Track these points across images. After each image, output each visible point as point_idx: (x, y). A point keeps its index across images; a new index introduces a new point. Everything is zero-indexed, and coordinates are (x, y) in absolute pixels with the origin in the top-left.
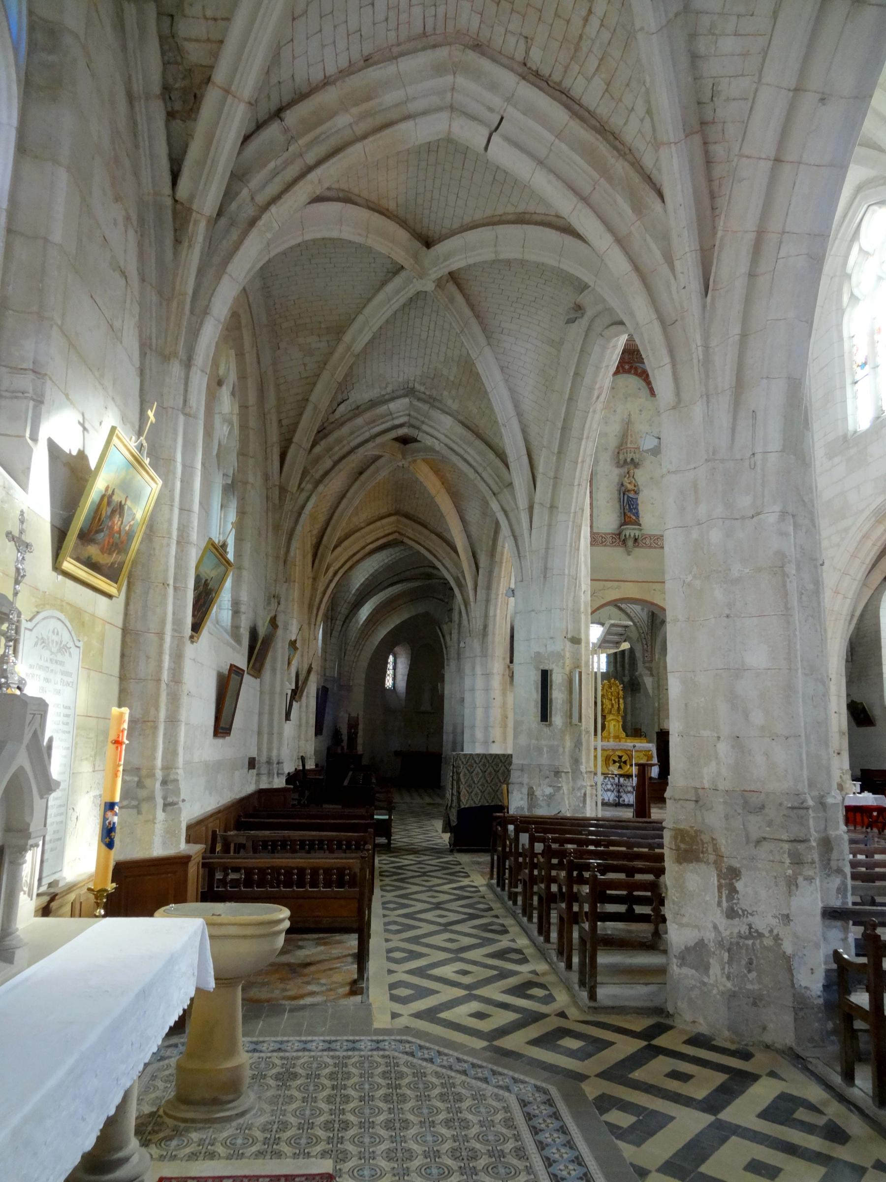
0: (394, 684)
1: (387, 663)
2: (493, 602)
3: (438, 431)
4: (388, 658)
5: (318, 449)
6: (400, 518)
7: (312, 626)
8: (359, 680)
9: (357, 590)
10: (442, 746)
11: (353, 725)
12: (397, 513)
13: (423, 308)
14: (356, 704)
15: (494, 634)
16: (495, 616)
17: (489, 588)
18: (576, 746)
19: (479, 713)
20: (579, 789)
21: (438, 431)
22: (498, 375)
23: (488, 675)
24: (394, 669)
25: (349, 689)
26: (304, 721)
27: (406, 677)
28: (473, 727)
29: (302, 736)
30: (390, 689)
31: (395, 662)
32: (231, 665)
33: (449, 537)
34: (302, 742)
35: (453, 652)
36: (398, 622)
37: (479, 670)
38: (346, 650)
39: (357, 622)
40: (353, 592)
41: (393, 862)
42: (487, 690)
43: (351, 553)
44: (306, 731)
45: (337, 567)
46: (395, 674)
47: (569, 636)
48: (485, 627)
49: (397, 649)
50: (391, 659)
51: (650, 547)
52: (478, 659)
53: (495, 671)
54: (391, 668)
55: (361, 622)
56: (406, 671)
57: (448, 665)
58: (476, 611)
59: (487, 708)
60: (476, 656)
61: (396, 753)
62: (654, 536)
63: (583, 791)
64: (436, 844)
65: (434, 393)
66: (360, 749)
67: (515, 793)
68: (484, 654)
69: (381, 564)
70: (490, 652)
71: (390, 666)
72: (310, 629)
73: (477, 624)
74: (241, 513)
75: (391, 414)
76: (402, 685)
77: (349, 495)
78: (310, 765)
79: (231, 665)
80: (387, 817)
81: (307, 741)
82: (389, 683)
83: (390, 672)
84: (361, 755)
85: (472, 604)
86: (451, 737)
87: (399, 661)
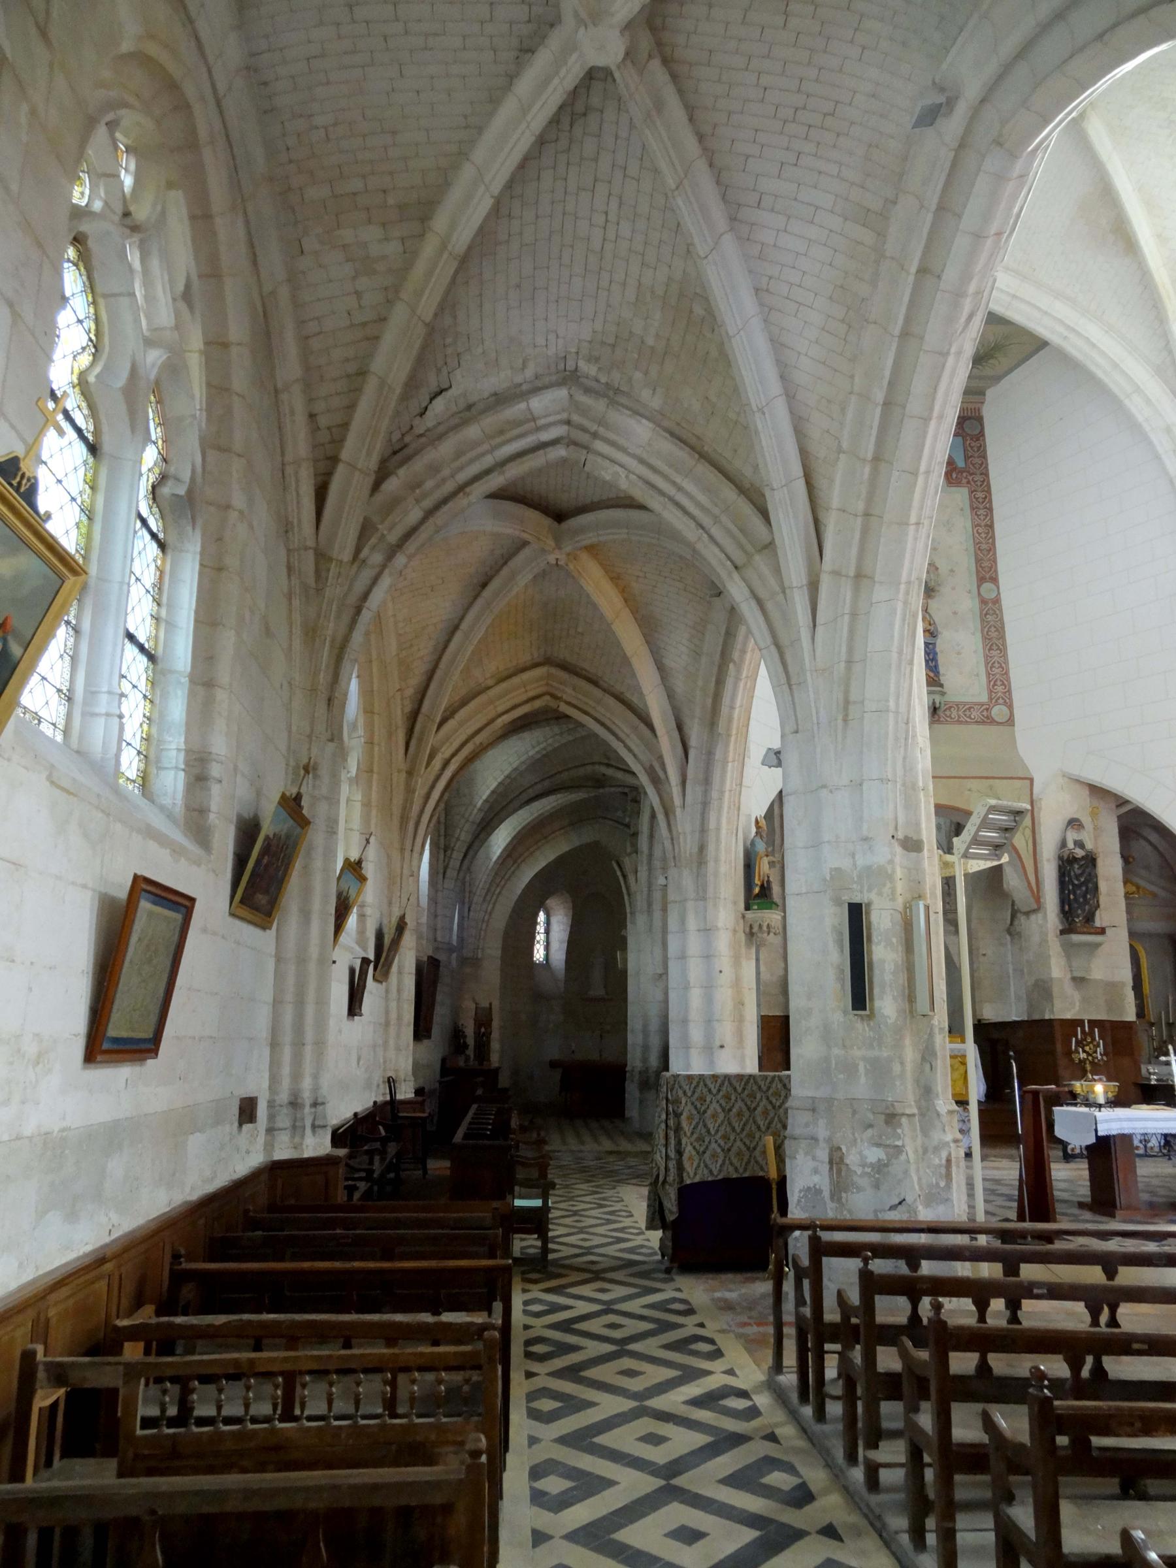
1: (535, 923)
2: (714, 804)
3: (624, 450)
4: (537, 915)
5: (392, 485)
6: (553, 670)
7: (407, 854)
8: (492, 950)
9: (486, 801)
10: (625, 1053)
11: (483, 1020)
12: (548, 661)
13: (596, 160)
14: (488, 987)
15: (717, 860)
16: (718, 829)
17: (707, 781)
18: (923, 1059)
19: (696, 997)
20: (937, 1149)
21: (624, 450)
22: (749, 304)
23: (707, 931)
24: (547, 932)
26: (393, 1016)
27: (565, 945)
28: (685, 1021)
29: (392, 1042)
30: (541, 964)
31: (548, 923)
32: (136, 878)
33: (635, 700)
34: (391, 1054)
35: (640, 901)
37: (692, 923)
39: (488, 858)
40: (479, 805)
41: (555, 1308)
42: (708, 957)
43: (470, 731)
44: (398, 1036)
45: (447, 755)
46: (549, 940)
47: (900, 835)
48: (702, 848)
49: (551, 902)
50: (541, 917)
51: (959, 722)
52: (690, 905)
53: (720, 924)
54: (542, 931)
56: (565, 936)
57: (634, 923)
58: (685, 823)
59: (709, 988)
60: (686, 900)
61: (553, 1064)
62: (965, 704)
63: (944, 1155)
64: (631, 1250)
65: (616, 377)
66: (495, 1059)
67: (800, 1157)
68: (702, 895)
69: (523, 759)
70: (710, 890)
71: (541, 928)
72: (403, 859)
73: (687, 845)
74: (213, 572)
75: (534, 420)
76: (559, 957)
77: (464, 626)
78: (406, 1092)
79: (136, 878)
80: (538, 1203)
81: (398, 1049)
82: (539, 954)
83: (540, 937)
84: (496, 1071)
85: (678, 811)
86: (639, 1039)
87: (554, 920)
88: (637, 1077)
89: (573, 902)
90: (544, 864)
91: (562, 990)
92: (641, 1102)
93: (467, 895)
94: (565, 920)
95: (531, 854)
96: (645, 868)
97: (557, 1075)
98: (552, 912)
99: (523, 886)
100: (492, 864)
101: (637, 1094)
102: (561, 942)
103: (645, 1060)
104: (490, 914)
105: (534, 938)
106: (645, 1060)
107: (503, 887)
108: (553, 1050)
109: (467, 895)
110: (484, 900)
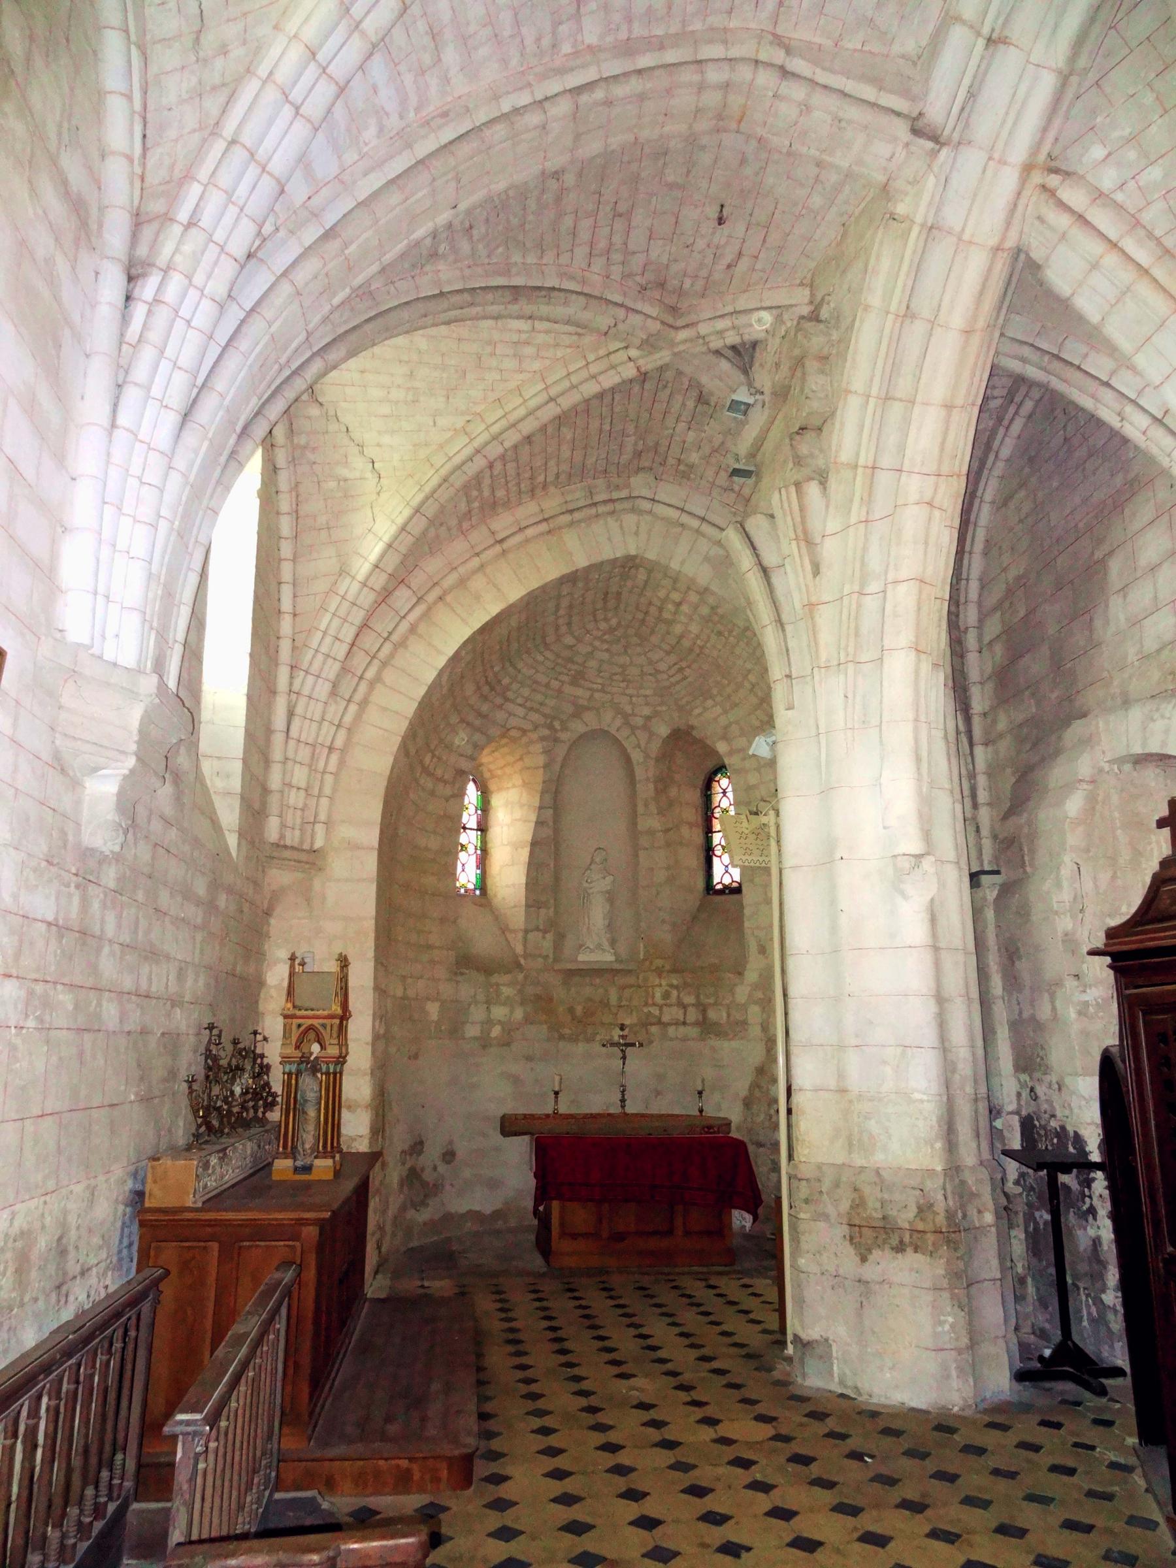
0: (483, 884)
24: (483, 828)
25: (311, 860)
27: (525, 853)
31: (485, 808)
36: (515, 593)
46: (497, 838)
54: (473, 823)
55: (362, 568)
56: (525, 833)
61: (510, 1126)
76: (510, 875)
82: (467, 875)
90: (494, 609)
91: (519, 949)
94: (525, 798)
97: (519, 1150)
98: (492, 786)
102: (516, 846)
108: (498, 1088)
110: (334, 693)
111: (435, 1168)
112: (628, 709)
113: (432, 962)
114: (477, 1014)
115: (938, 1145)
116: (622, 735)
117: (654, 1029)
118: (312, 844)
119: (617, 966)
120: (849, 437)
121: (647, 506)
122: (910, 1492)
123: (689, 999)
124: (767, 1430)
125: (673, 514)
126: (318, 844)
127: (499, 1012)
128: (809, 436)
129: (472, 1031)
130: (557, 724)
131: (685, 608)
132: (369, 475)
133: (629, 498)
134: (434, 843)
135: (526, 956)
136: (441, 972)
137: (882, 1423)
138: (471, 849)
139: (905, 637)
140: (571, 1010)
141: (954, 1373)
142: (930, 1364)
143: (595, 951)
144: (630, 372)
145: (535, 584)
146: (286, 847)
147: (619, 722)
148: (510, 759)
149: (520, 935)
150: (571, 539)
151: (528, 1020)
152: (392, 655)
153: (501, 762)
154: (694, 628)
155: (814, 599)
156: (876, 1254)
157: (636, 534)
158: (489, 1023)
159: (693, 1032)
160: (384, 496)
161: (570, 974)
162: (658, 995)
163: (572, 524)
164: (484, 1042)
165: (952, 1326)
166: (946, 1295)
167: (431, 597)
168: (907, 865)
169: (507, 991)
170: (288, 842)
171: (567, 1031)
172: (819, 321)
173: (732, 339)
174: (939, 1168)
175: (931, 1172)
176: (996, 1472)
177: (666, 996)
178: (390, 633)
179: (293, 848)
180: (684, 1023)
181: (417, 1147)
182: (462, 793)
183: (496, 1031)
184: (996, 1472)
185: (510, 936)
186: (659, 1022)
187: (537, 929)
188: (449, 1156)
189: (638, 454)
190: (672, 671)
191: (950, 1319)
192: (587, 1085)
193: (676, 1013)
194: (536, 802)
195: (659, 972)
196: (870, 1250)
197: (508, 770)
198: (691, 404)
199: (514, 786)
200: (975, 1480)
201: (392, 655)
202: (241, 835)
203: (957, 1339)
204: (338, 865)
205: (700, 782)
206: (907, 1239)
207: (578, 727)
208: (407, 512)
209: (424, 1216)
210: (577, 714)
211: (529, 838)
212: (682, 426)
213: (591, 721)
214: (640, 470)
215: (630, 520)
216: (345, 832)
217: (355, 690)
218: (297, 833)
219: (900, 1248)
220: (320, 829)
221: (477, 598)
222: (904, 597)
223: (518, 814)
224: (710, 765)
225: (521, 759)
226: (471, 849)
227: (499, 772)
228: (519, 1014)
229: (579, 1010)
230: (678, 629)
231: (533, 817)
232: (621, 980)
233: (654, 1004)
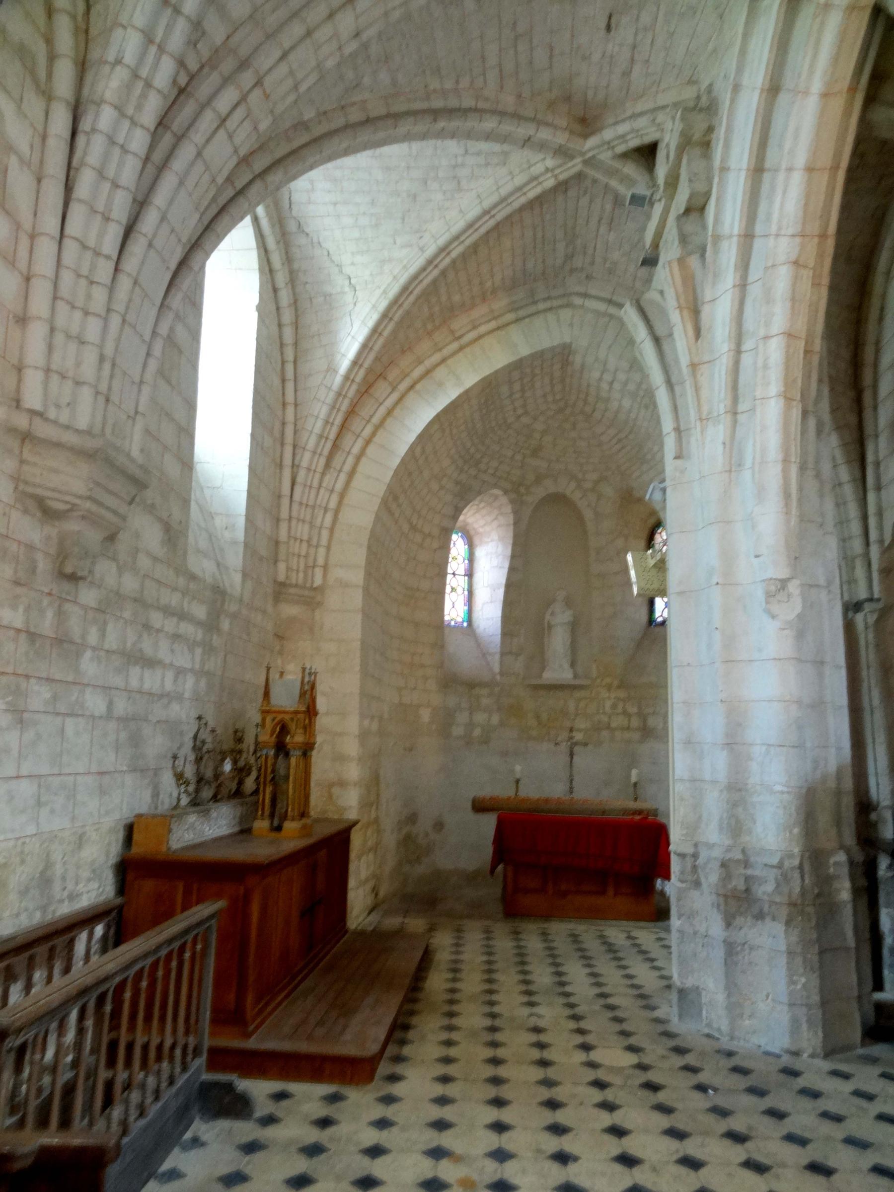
25: (312, 598)
27: (501, 593)
30: (458, 627)
31: (471, 559)
36: (470, 379)
38: (295, 466)
39: (331, 369)
46: (477, 580)
50: (458, 546)
54: (461, 570)
55: (344, 365)
61: (480, 807)
76: (489, 614)
83: (455, 583)
86: (717, 765)
87: (481, 553)
88: (712, 877)
89: (516, 512)
91: (497, 668)
92: (731, 949)
93: (288, 450)
94: (500, 549)
95: (428, 372)
96: (729, 279)
97: (489, 823)
98: (476, 540)
99: (412, 437)
100: (338, 380)
101: (716, 927)
102: (494, 588)
103: (736, 827)
104: (342, 496)
105: (442, 574)
106: (736, 827)
107: (368, 442)
109: (288, 450)
110: (328, 465)
111: (427, 835)
112: (580, 476)
113: (426, 678)
114: (462, 718)
115: (796, 831)
116: (576, 496)
117: (605, 734)
118: (313, 583)
119: (573, 682)
120: (728, 212)
121: (578, 301)
122: (737, 1124)
123: (633, 710)
124: (632, 1059)
125: (602, 307)
126: (318, 581)
127: (480, 717)
128: (694, 216)
129: (458, 731)
130: (522, 490)
131: (617, 386)
132: (347, 289)
133: (564, 295)
134: (425, 585)
135: (502, 674)
136: (432, 685)
137: (735, 1061)
138: (459, 590)
139: (775, 387)
140: (538, 717)
141: (805, 1027)
142: (783, 1016)
143: (558, 671)
144: (550, 183)
145: (487, 371)
146: (291, 586)
147: (573, 485)
148: (489, 519)
149: (497, 657)
150: (515, 334)
151: (502, 724)
152: (374, 434)
153: (482, 522)
154: (626, 403)
155: (696, 360)
156: (739, 921)
157: (571, 325)
158: (470, 725)
159: (636, 736)
160: (358, 305)
161: (536, 687)
162: (608, 704)
163: (517, 320)
164: (468, 741)
165: (804, 985)
166: (799, 960)
167: (403, 387)
168: (773, 588)
169: (485, 701)
170: (294, 581)
171: (534, 733)
172: (701, 110)
173: (634, 143)
174: (796, 850)
175: (791, 856)
176: (825, 1115)
177: (614, 706)
178: (371, 416)
179: (296, 586)
180: (628, 728)
181: (412, 818)
182: (445, 547)
183: (477, 732)
184: (825, 1115)
185: (489, 658)
186: (608, 727)
187: (510, 653)
188: (439, 826)
189: (569, 257)
190: (614, 441)
191: (803, 980)
192: (542, 776)
193: (618, 721)
194: (509, 552)
195: (609, 687)
196: (734, 917)
197: (487, 528)
198: (608, 207)
199: (492, 541)
200: (803, 1118)
201: (374, 434)
202: (245, 575)
203: (808, 997)
204: (333, 599)
205: (645, 534)
206: (766, 908)
207: (540, 492)
208: (375, 317)
209: (420, 870)
210: (539, 479)
211: (504, 581)
212: (603, 229)
213: (550, 487)
214: (572, 271)
215: (566, 314)
216: (337, 573)
217: (344, 463)
218: (301, 575)
219: (760, 916)
220: (319, 572)
221: (440, 385)
222: (775, 351)
223: (495, 562)
224: (652, 521)
225: (495, 519)
226: (459, 590)
227: (481, 530)
228: (495, 719)
229: (544, 717)
230: (615, 405)
231: (507, 565)
232: (578, 694)
233: (604, 713)
